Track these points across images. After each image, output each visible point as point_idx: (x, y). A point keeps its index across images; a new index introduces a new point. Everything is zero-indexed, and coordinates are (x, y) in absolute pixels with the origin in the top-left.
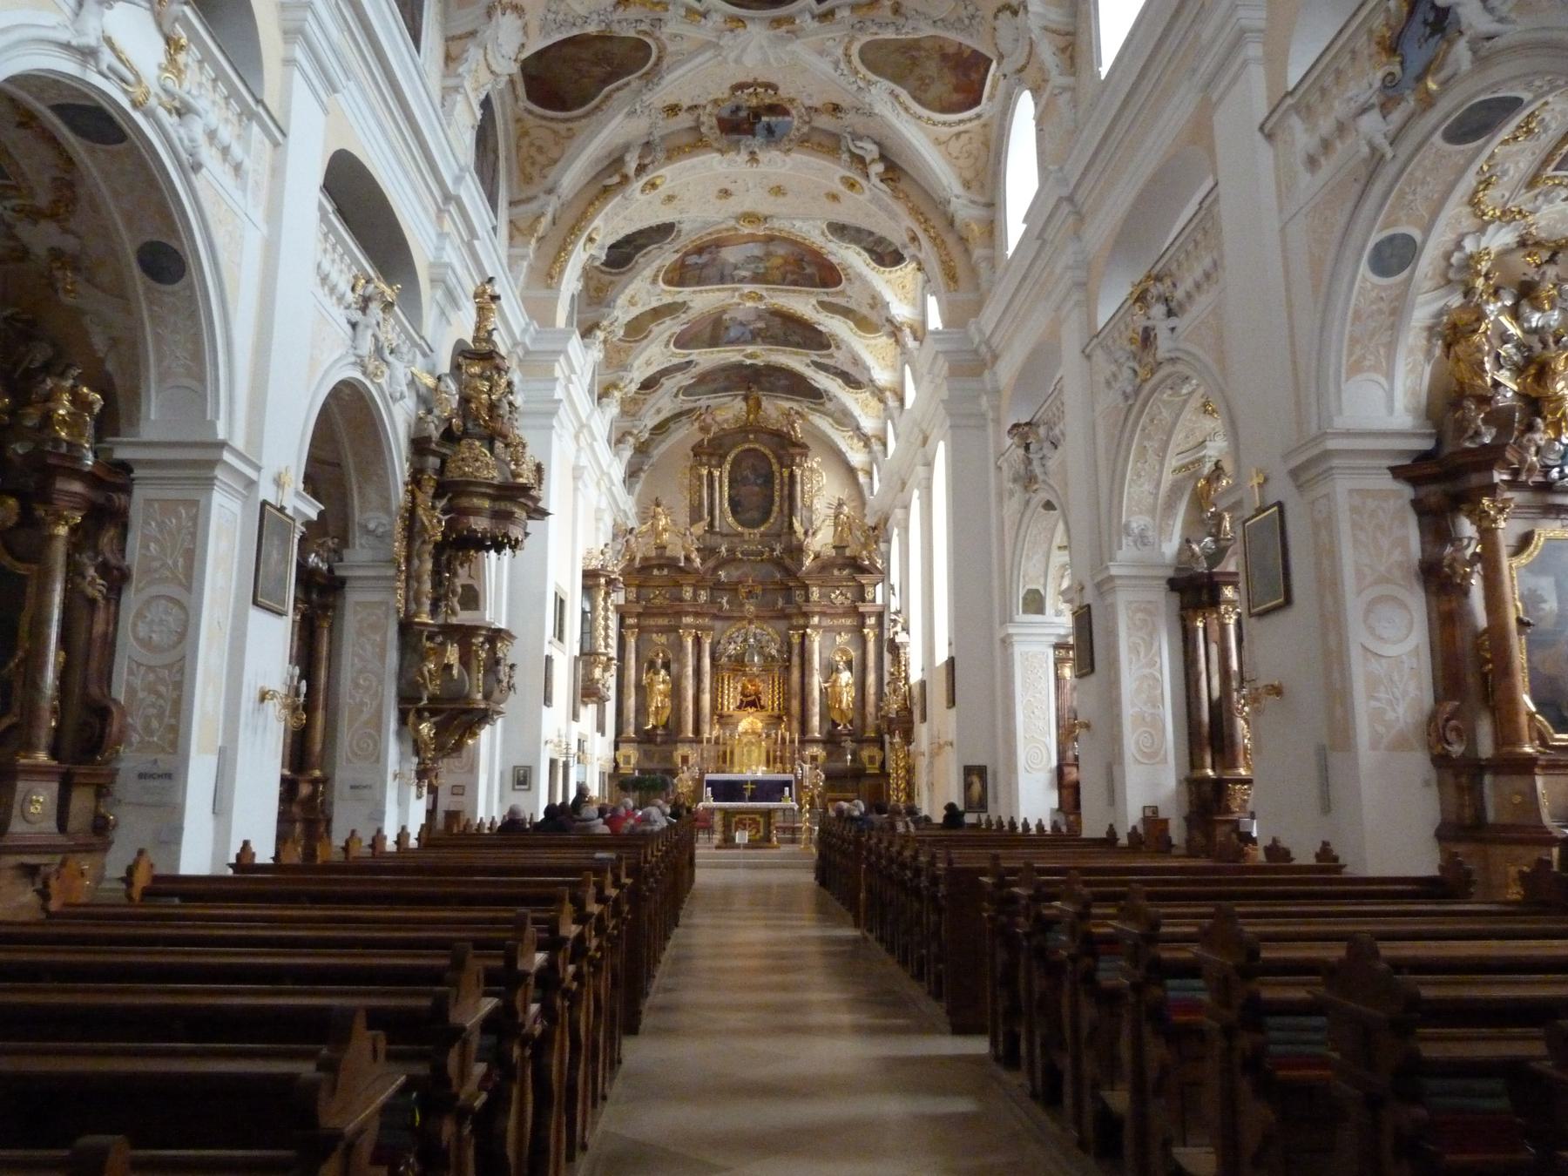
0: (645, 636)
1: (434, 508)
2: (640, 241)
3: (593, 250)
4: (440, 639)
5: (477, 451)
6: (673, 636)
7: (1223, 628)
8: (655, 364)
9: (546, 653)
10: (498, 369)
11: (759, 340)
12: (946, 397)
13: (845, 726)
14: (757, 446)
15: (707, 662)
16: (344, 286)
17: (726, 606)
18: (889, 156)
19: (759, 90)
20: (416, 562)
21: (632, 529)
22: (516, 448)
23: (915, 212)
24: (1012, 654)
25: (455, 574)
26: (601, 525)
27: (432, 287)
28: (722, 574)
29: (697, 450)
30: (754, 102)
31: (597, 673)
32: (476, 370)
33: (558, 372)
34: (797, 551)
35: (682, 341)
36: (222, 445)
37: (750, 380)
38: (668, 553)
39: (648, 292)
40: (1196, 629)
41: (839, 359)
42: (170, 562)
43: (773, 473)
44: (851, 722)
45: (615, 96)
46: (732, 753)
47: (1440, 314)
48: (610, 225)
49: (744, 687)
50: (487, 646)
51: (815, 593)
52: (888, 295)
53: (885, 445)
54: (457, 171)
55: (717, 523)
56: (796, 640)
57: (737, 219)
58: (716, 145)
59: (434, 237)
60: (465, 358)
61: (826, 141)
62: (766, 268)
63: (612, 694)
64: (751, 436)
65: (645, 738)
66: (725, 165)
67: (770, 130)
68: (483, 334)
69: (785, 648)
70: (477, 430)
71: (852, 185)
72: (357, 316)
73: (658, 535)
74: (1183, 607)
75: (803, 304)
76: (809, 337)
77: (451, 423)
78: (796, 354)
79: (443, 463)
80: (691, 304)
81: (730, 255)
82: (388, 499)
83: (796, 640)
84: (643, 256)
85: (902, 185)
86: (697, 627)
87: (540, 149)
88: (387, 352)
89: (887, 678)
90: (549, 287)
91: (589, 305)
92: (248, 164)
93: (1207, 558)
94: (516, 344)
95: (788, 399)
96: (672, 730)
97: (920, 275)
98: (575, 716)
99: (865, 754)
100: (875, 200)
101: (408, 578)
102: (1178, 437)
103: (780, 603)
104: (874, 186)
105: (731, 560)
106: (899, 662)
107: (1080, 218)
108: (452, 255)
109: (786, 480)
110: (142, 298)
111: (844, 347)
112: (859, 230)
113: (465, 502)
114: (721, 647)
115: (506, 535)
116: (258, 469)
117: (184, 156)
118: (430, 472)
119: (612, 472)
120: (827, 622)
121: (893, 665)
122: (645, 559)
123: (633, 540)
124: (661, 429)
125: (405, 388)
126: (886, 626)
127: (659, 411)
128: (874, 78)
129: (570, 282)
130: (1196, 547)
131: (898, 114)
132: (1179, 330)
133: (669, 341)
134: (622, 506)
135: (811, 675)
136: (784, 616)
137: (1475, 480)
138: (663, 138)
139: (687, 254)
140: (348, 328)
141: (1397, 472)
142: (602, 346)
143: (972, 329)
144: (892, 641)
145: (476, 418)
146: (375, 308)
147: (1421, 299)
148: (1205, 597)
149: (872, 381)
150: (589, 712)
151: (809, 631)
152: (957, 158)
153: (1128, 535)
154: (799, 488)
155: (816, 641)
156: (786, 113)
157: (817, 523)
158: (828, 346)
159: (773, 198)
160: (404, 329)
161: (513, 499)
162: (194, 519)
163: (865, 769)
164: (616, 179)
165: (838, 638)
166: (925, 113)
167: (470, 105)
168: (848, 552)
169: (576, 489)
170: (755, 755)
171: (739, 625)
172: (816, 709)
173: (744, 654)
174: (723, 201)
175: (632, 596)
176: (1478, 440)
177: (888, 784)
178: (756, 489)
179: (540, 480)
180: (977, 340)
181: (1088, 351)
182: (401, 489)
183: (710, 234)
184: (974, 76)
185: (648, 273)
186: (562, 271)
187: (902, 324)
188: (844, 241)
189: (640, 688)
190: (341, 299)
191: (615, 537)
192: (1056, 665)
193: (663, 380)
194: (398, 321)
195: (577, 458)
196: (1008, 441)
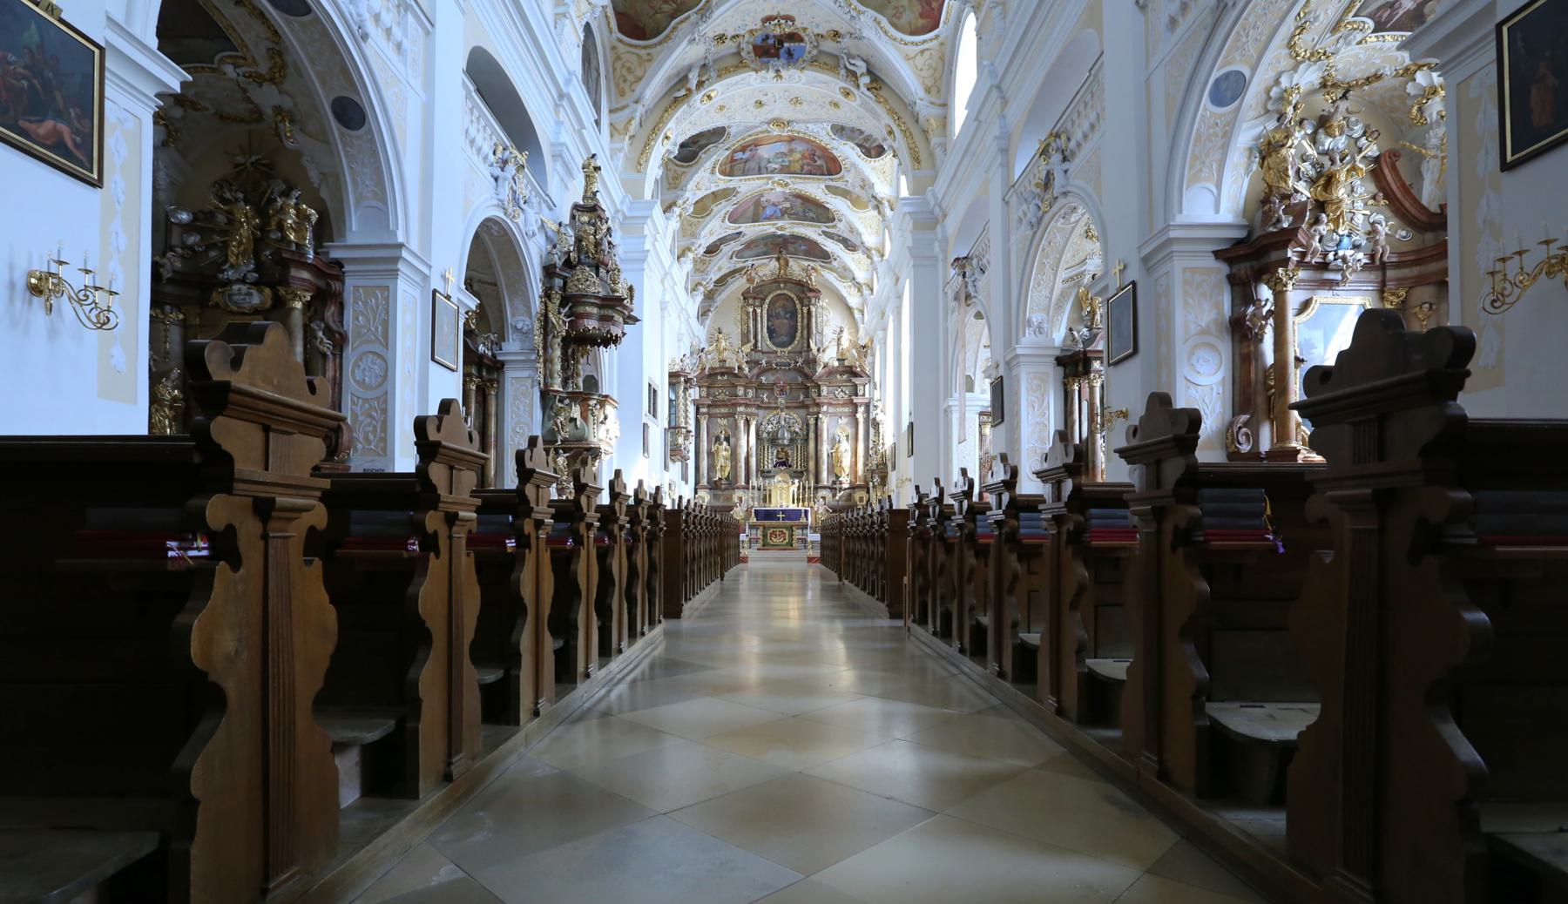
1: (560, 313)
2: (703, 142)
3: (668, 145)
4: (567, 401)
5: (587, 274)
6: (731, 419)
7: (1092, 388)
8: (716, 233)
9: (644, 420)
10: (601, 219)
11: (786, 216)
12: (911, 245)
14: (786, 292)
16: (487, 149)
17: (766, 400)
18: (873, 70)
19: (782, 21)
20: (550, 350)
21: (703, 349)
22: (614, 272)
23: (891, 112)
24: (951, 419)
25: (578, 362)
26: (682, 345)
27: (554, 161)
28: (763, 378)
29: (746, 295)
30: (778, 31)
31: (680, 440)
32: (585, 218)
33: (646, 232)
34: (812, 362)
35: (734, 218)
36: (401, 246)
37: (780, 246)
38: (727, 365)
39: (709, 180)
40: (1073, 391)
41: (841, 228)
42: (373, 329)
45: (680, 27)
46: (770, 496)
47: (1259, 137)
48: (680, 128)
50: (598, 407)
51: (824, 390)
52: (873, 178)
53: (872, 290)
54: (566, 73)
55: (759, 344)
56: (812, 422)
57: (769, 123)
58: (752, 66)
59: (552, 122)
60: (578, 211)
61: (829, 61)
62: (790, 162)
63: (692, 455)
64: (782, 285)
65: (714, 486)
66: (758, 81)
67: (790, 54)
68: (589, 194)
70: (588, 260)
71: (847, 94)
72: (497, 172)
73: (720, 353)
74: (1066, 376)
75: (815, 188)
76: (818, 213)
77: (569, 255)
78: (812, 226)
79: (565, 283)
80: (739, 190)
81: (765, 152)
82: (529, 308)
83: (812, 422)
84: (705, 153)
85: (882, 93)
86: (747, 414)
87: (629, 70)
88: (522, 202)
89: (871, 445)
90: (639, 172)
91: (668, 189)
92: (406, 44)
93: (1083, 342)
94: (617, 211)
95: (806, 260)
96: (731, 482)
97: (896, 161)
98: (666, 467)
99: (858, 495)
100: (863, 104)
101: (545, 362)
102: (1068, 255)
103: (802, 397)
104: (862, 95)
105: (768, 369)
106: (879, 433)
107: (1005, 101)
108: (567, 137)
109: (805, 315)
110: (339, 142)
111: (844, 220)
112: (853, 130)
113: (581, 309)
115: (608, 332)
116: (430, 267)
117: (355, 28)
118: (557, 289)
119: (688, 307)
120: (831, 410)
121: (875, 436)
122: (712, 369)
124: (721, 282)
125: (535, 228)
126: (871, 410)
127: (720, 269)
128: (862, 8)
129: (654, 170)
130: (1075, 333)
131: (880, 36)
132: (1069, 172)
133: (725, 217)
135: (822, 445)
136: (804, 406)
137: (1275, 256)
138: (715, 61)
139: (735, 151)
140: (493, 180)
141: (1218, 255)
142: (678, 219)
143: (929, 196)
144: (874, 419)
145: (587, 253)
146: (511, 168)
147: (1245, 126)
148: (1080, 368)
149: (862, 243)
150: (676, 468)
151: (820, 415)
152: (921, 70)
153: (1031, 327)
154: (814, 320)
155: (825, 422)
156: (801, 40)
157: (826, 344)
158: (834, 220)
159: (792, 107)
160: (534, 188)
161: (612, 307)
162: (387, 299)
164: (683, 92)
165: (840, 420)
166: (899, 35)
167: (575, 28)
168: (846, 363)
169: (663, 317)
174: (759, 110)
175: (704, 394)
176: (1278, 226)
178: (785, 321)
179: (632, 297)
180: (932, 203)
181: (1006, 199)
182: (538, 301)
183: (750, 136)
184: (935, 5)
185: (709, 165)
186: (647, 161)
187: (883, 198)
188: (841, 139)
189: (710, 454)
190: (485, 158)
191: (692, 354)
192: (980, 426)
193: (722, 246)
194: (529, 182)
195: (664, 295)
196: (952, 272)
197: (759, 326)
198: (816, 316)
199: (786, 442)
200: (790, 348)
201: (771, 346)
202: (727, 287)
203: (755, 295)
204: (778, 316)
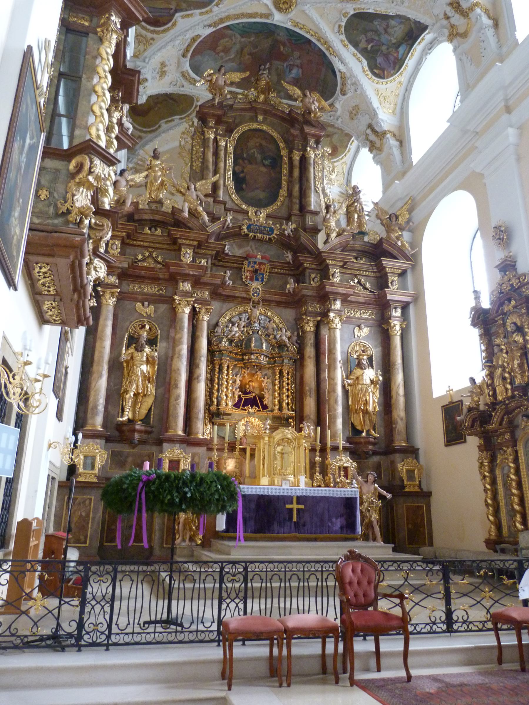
0: (127, 303)
6: (163, 308)
13: (368, 432)
17: (229, 282)
43: (281, 157)
56: (310, 327)
64: (260, 118)
109: (296, 163)
170: (292, 458)
172: (340, 410)
201: (239, 202)
202: (156, 137)
203: (220, 113)
204: (251, 160)
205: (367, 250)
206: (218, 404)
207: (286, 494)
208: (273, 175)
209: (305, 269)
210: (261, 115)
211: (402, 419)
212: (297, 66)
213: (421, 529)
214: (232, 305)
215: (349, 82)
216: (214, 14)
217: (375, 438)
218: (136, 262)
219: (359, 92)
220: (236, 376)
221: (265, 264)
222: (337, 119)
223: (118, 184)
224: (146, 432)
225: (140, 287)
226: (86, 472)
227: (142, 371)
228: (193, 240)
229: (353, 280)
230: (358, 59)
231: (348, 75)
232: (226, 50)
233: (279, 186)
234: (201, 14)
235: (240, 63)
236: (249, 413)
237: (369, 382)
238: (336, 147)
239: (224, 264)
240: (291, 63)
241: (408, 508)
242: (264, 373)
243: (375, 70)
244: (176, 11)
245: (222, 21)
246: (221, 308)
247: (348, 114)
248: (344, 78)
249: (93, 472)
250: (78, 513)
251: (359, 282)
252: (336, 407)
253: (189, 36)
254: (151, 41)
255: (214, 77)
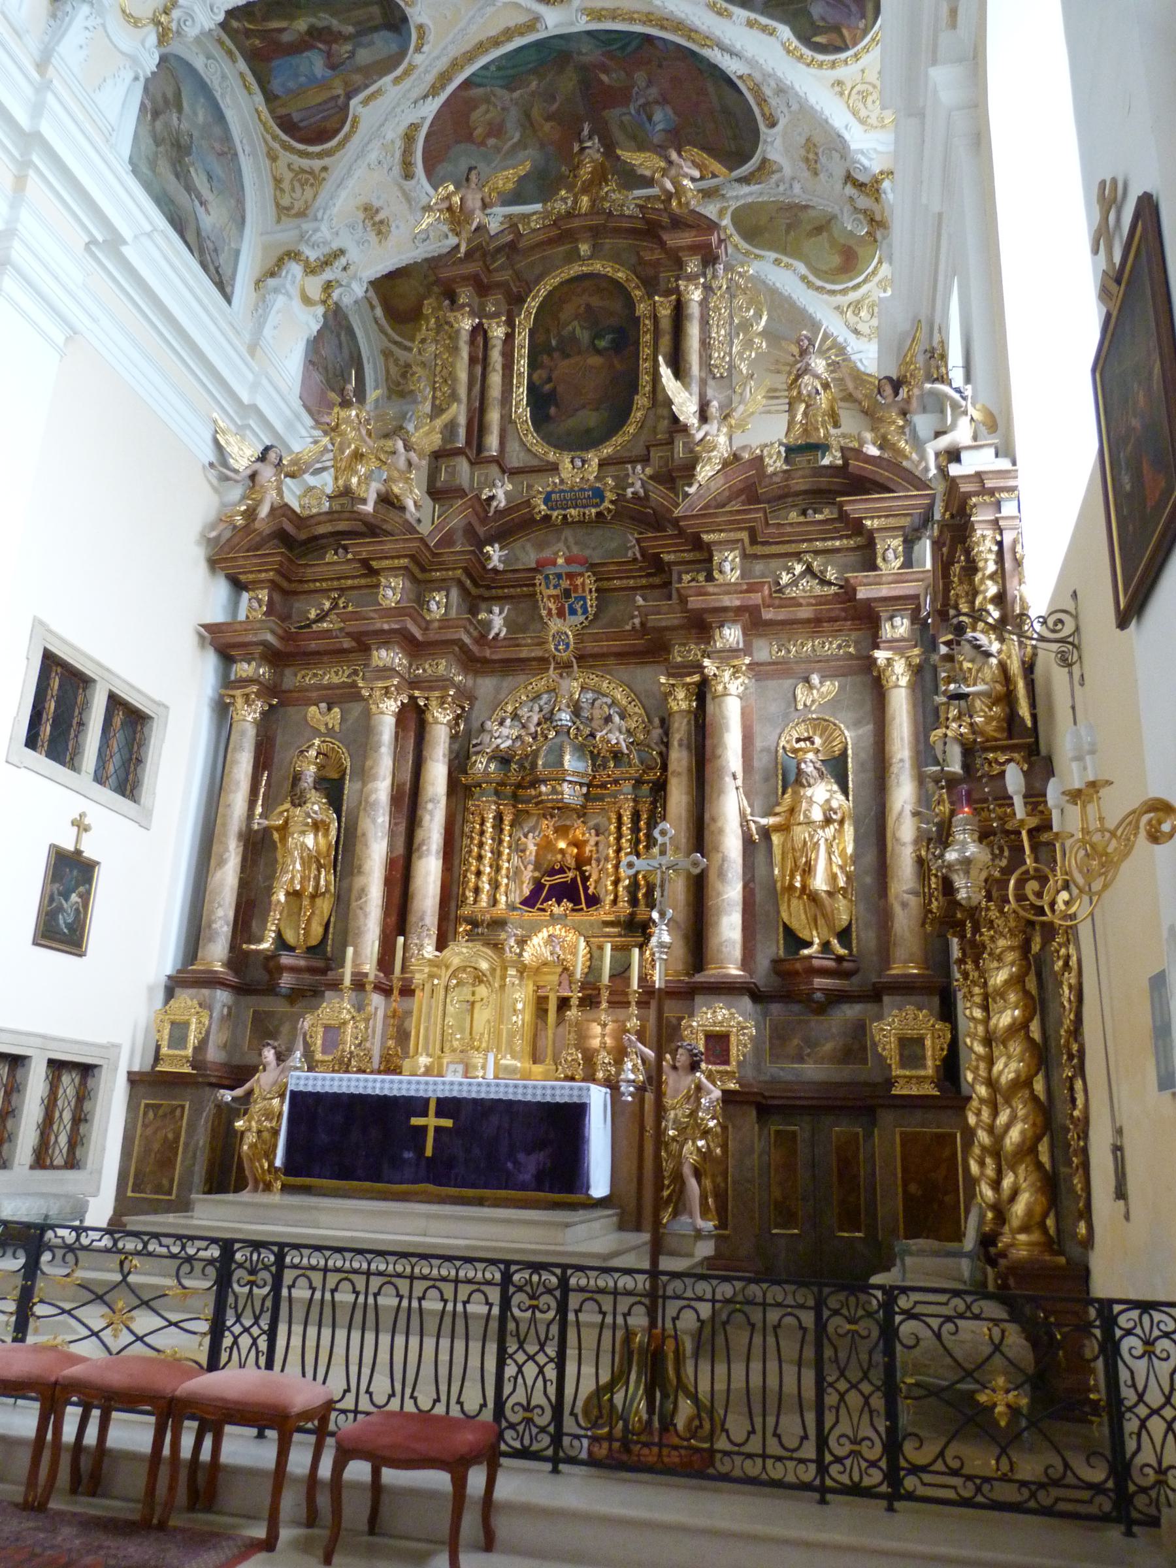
0: (291, 710)
6: (356, 709)
13: (826, 946)
14: (598, 267)
15: (437, 774)
28: (495, 554)
43: (636, 321)
44: (844, 935)
49: (546, 846)
51: (730, 565)
55: (493, 442)
56: (681, 702)
64: (584, 248)
69: (657, 733)
109: (666, 324)
114: (486, 738)
120: (765, 651)
123: (267, 473)
134: (246, 399)
151: (707, 662)
154: (693, 331)
163: (890, 1083)
170: (483, 1016)
171: (539, 684)
173: (535, 754)
177: (969, 1134)
178: (595, 361)
197: (496, 379)
198: (705, 323)
199: (570, 793)
200: (607, 451)
204: (568, 347)
205: (823, 486)
206: (475, 902)
207: (412, 1093)
208: (618, 366)
209: (670, 564)
210: (584, 242)
211: (904, 905)
212: (657, 102)
213: (947, 1199)
214: (521, 678)
215: (768, 92)
216: (421, 69)
217: (840, 959)
218: (308, 626)
219: (795, 107)
220: (526, 836)
221: (581, 575)
222: (791, 186)
223: (258, 478)
224: (311, 970)
225: (315, 675)
226: (171, 1052)
227: (304, 846)
228: (398, 557)
229: (789, 570)
230: (764, 29)
231: (758, 76)
232: (496, 130)
233: (634, 388)
234: (397, 81)
235: (542, 146)
236: (552, 915)
237: (817, 815)
238: (850, 248)
239: (500, 592)
240: (641, 101)
241: (906, 1140)
242: (591, 823)
243: (818, 39)
244: (349, 97)
245: (444, 78)
246: (498, 690)
247: (803, 166)
248: (757, 91)
249: (182, 1053)
250: (161, 1135)
251: (809, 570)
252: (719, 886)
253: (394, 133)
254: (323, 175)
255: (456, 199)
